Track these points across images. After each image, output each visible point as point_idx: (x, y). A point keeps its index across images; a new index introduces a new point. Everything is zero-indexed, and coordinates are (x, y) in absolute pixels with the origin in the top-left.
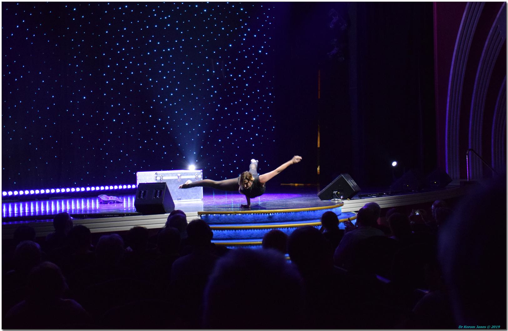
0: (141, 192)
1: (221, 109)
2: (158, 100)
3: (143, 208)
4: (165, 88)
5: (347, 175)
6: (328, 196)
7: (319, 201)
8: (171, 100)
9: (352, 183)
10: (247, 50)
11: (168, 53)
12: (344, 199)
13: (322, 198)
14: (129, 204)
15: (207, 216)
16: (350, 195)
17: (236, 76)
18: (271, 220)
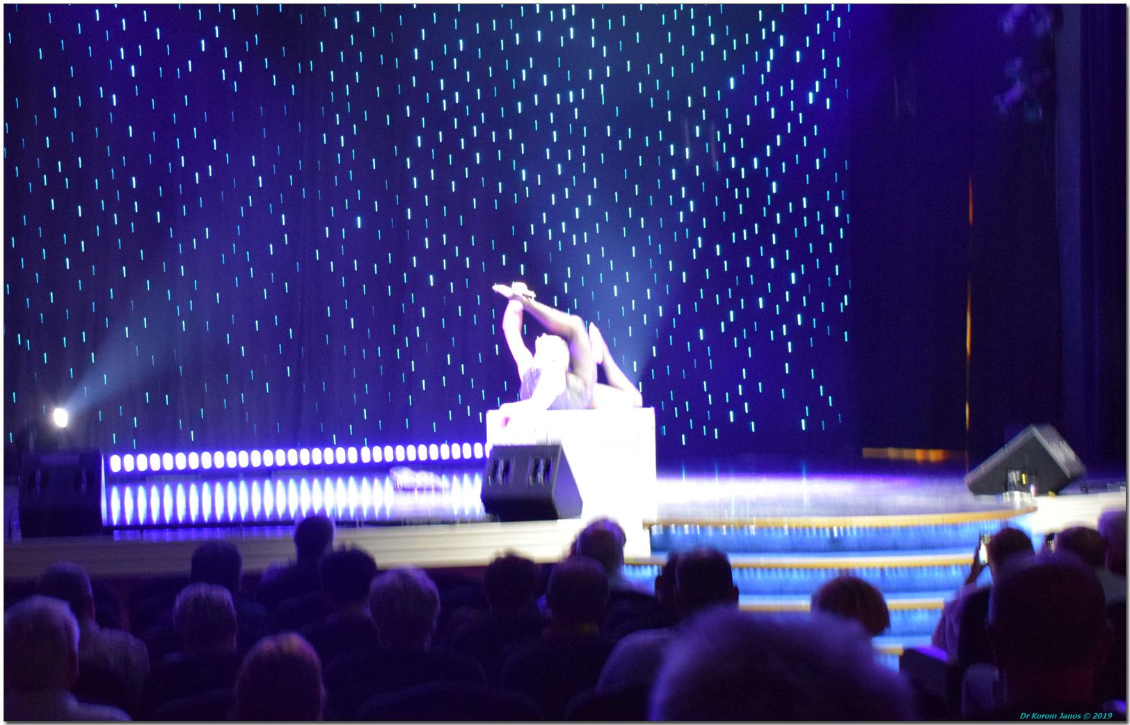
0: (496, 466)
1: (708, 250)
2: (541, 230)
3: (503, 507)
4: (560, 196)
5: (1050, 430)
6: (996, 485)
7: (968, 498)
8: (575, 227)
9: (1062, 453)
10: (775, 94)
11: (566, 107)
12: (1041, 492)
13: (977, 489)
14: (466, 494)
15: (666, 529)
16: (1056, 483)
17: (744, 161)
18: (836, 545)
